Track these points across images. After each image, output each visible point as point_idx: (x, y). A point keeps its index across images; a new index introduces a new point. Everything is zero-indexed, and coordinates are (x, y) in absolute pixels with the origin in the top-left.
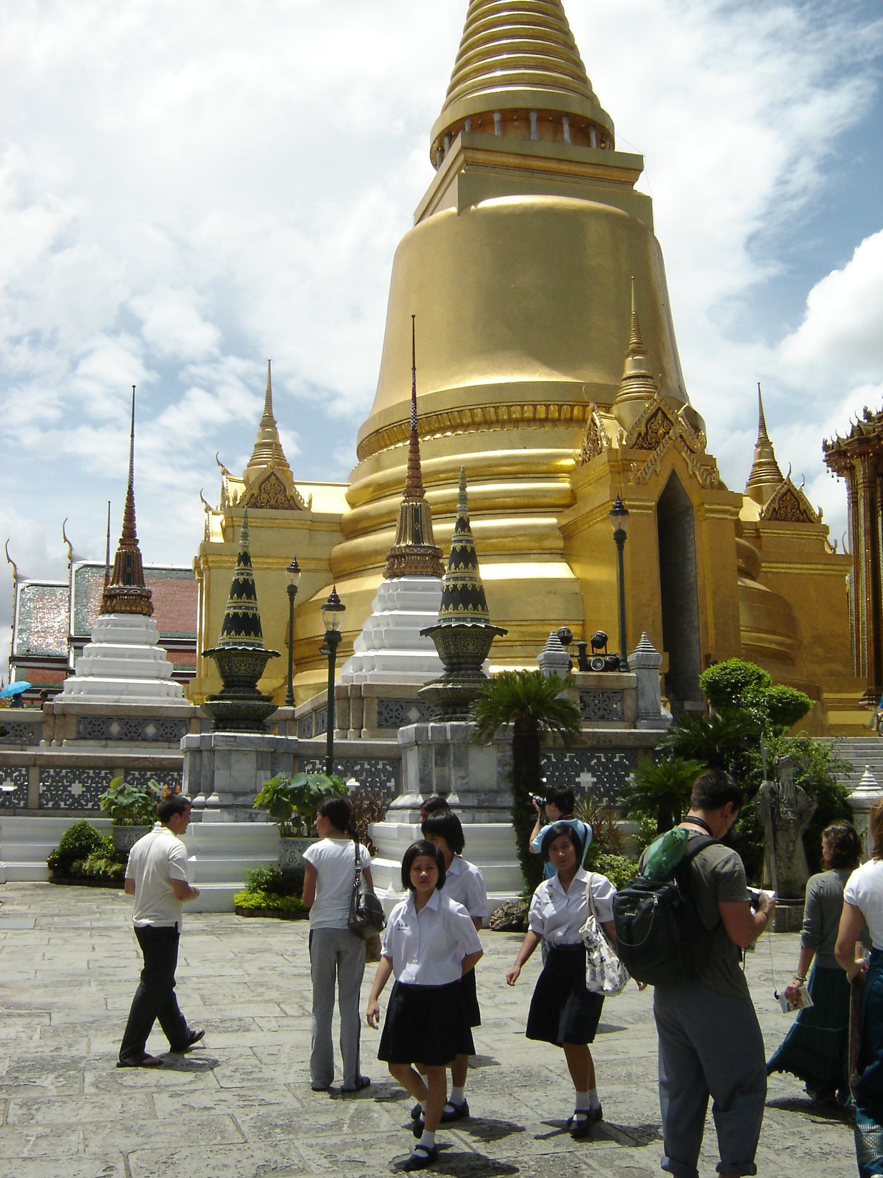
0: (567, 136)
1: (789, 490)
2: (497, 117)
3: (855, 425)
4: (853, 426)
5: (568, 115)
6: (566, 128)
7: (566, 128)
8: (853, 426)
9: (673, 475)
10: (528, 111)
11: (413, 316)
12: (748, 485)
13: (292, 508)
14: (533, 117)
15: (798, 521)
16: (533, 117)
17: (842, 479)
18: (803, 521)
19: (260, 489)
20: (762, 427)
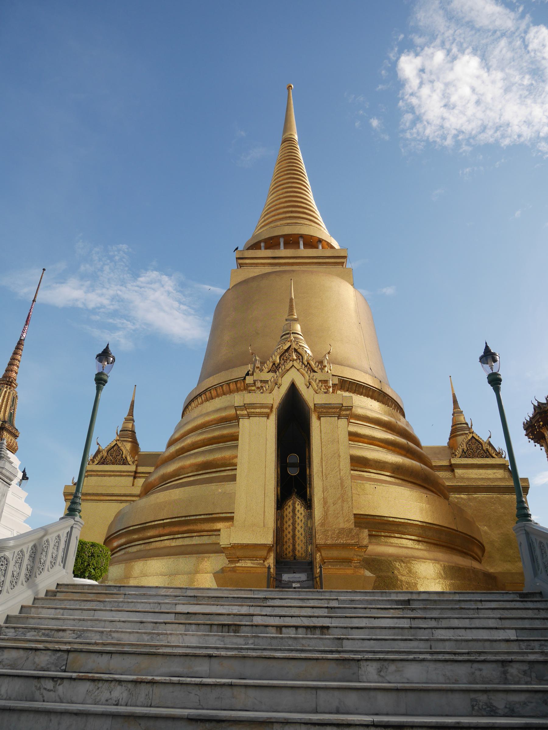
0: (302, 246)
1: (473, 437)
2: (262, 244)
3: (536, 404)
4: (534, 406)
5: (302, 236)
6: (301, 243)
7: (301, 243)
8: (534, 406)
9: (293, 388)
10: (278, 237)
11: (44, 270)
12: (449, 439)
13: (124, 464)
14: (282, 241)
15: (483, 457)
16: (282, 241)
17: (543, 448)
18: (486, 457)
19: (107, 454)
20: (455, 402)
